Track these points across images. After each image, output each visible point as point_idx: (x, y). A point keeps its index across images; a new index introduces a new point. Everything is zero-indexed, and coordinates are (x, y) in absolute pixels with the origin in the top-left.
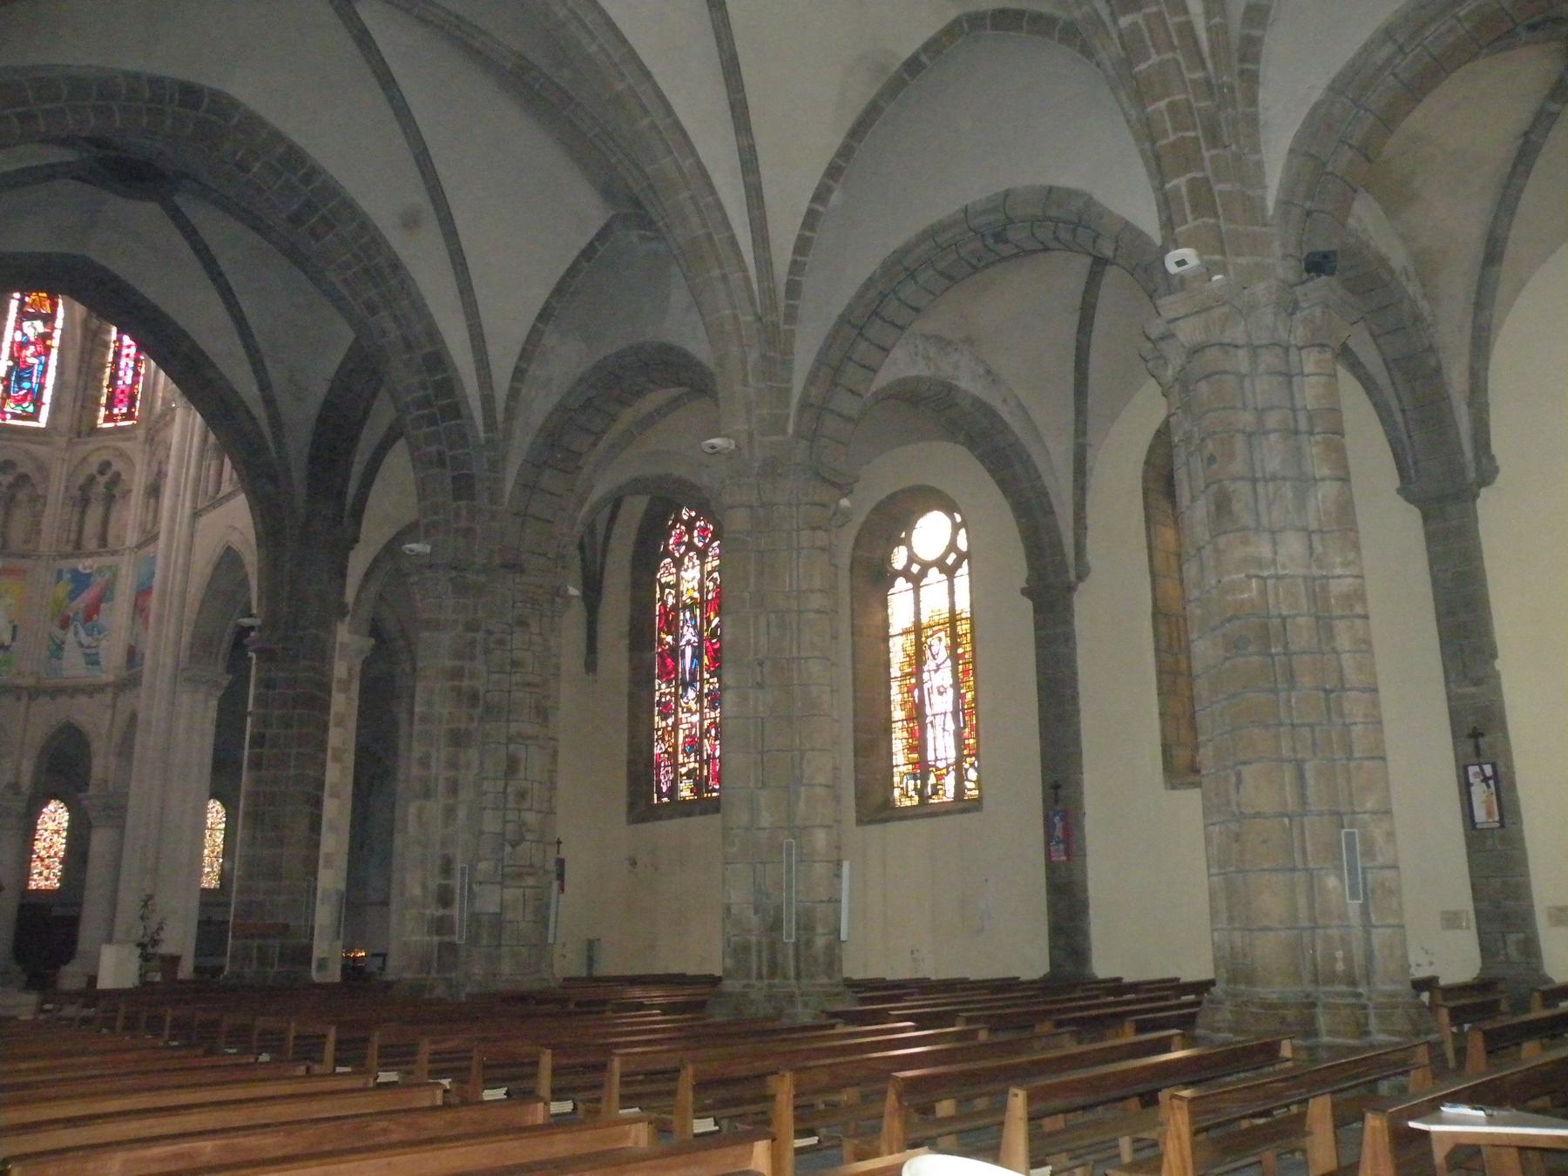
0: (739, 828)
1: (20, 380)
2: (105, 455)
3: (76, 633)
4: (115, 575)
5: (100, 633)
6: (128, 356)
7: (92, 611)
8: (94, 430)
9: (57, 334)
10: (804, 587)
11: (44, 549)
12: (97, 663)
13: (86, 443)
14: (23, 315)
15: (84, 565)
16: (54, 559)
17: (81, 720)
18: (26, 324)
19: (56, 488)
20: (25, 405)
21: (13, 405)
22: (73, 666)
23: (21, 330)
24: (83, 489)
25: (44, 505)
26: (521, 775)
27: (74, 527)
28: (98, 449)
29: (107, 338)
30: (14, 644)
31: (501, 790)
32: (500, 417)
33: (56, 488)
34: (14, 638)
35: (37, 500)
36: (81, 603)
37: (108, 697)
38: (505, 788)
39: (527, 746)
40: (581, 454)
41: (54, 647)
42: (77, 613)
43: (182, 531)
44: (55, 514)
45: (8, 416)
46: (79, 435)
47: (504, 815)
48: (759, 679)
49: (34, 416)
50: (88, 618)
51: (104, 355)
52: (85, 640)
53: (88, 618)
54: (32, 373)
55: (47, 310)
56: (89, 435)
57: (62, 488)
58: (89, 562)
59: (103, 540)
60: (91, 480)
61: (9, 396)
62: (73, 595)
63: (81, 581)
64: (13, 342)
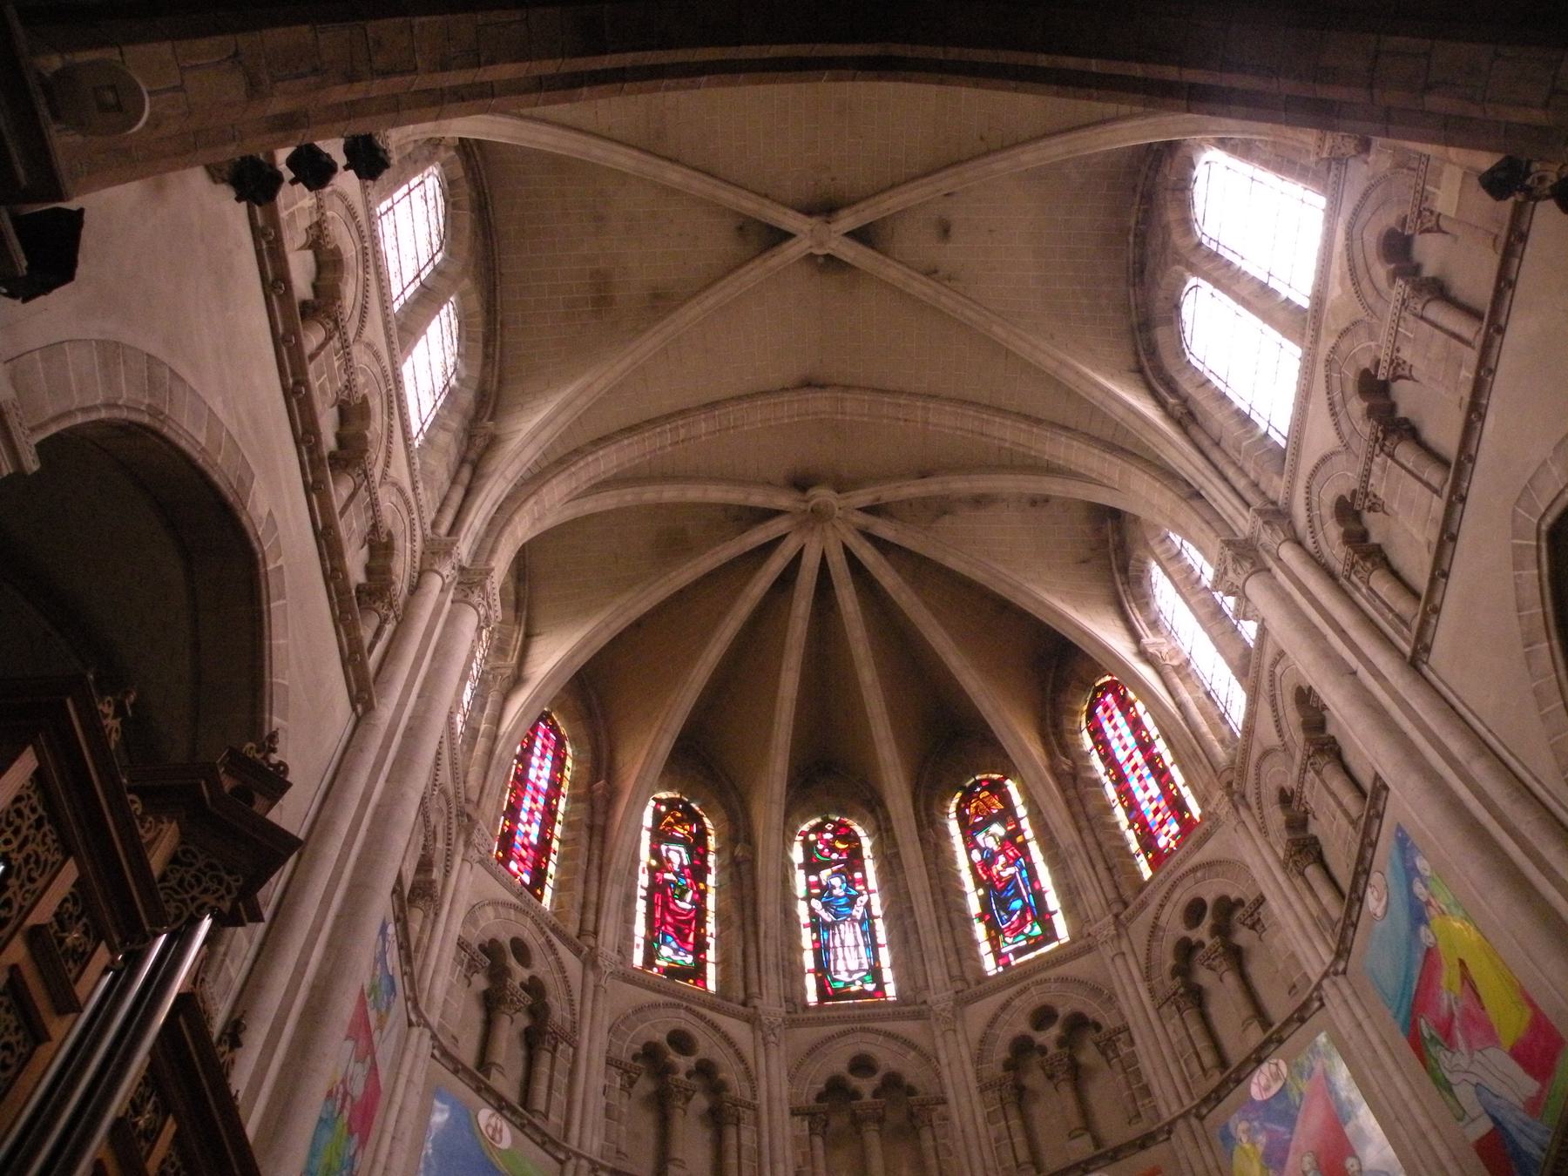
1: (1004, 904)
6: (1135, 768)
9: (1025, 824)
11: (1169, 1108)
14: (969, 831)
16: (1201, 1118)
18: (980, 838)
20: (1026, 930)
21: (1009, 940)
23: (977, 846)
25: (1132, 1042)
27: (1202, 1044)
29: (1095, 776)
35: (1113, 1041)
43: (1418, 702)
45: (1011, 957)
49: (1049, 934)
51: (1101, 795)
54: (1017, 887)
55: (997, 807)
57: (1145, 996)
61: (1000, 931)
64: (973, 867)
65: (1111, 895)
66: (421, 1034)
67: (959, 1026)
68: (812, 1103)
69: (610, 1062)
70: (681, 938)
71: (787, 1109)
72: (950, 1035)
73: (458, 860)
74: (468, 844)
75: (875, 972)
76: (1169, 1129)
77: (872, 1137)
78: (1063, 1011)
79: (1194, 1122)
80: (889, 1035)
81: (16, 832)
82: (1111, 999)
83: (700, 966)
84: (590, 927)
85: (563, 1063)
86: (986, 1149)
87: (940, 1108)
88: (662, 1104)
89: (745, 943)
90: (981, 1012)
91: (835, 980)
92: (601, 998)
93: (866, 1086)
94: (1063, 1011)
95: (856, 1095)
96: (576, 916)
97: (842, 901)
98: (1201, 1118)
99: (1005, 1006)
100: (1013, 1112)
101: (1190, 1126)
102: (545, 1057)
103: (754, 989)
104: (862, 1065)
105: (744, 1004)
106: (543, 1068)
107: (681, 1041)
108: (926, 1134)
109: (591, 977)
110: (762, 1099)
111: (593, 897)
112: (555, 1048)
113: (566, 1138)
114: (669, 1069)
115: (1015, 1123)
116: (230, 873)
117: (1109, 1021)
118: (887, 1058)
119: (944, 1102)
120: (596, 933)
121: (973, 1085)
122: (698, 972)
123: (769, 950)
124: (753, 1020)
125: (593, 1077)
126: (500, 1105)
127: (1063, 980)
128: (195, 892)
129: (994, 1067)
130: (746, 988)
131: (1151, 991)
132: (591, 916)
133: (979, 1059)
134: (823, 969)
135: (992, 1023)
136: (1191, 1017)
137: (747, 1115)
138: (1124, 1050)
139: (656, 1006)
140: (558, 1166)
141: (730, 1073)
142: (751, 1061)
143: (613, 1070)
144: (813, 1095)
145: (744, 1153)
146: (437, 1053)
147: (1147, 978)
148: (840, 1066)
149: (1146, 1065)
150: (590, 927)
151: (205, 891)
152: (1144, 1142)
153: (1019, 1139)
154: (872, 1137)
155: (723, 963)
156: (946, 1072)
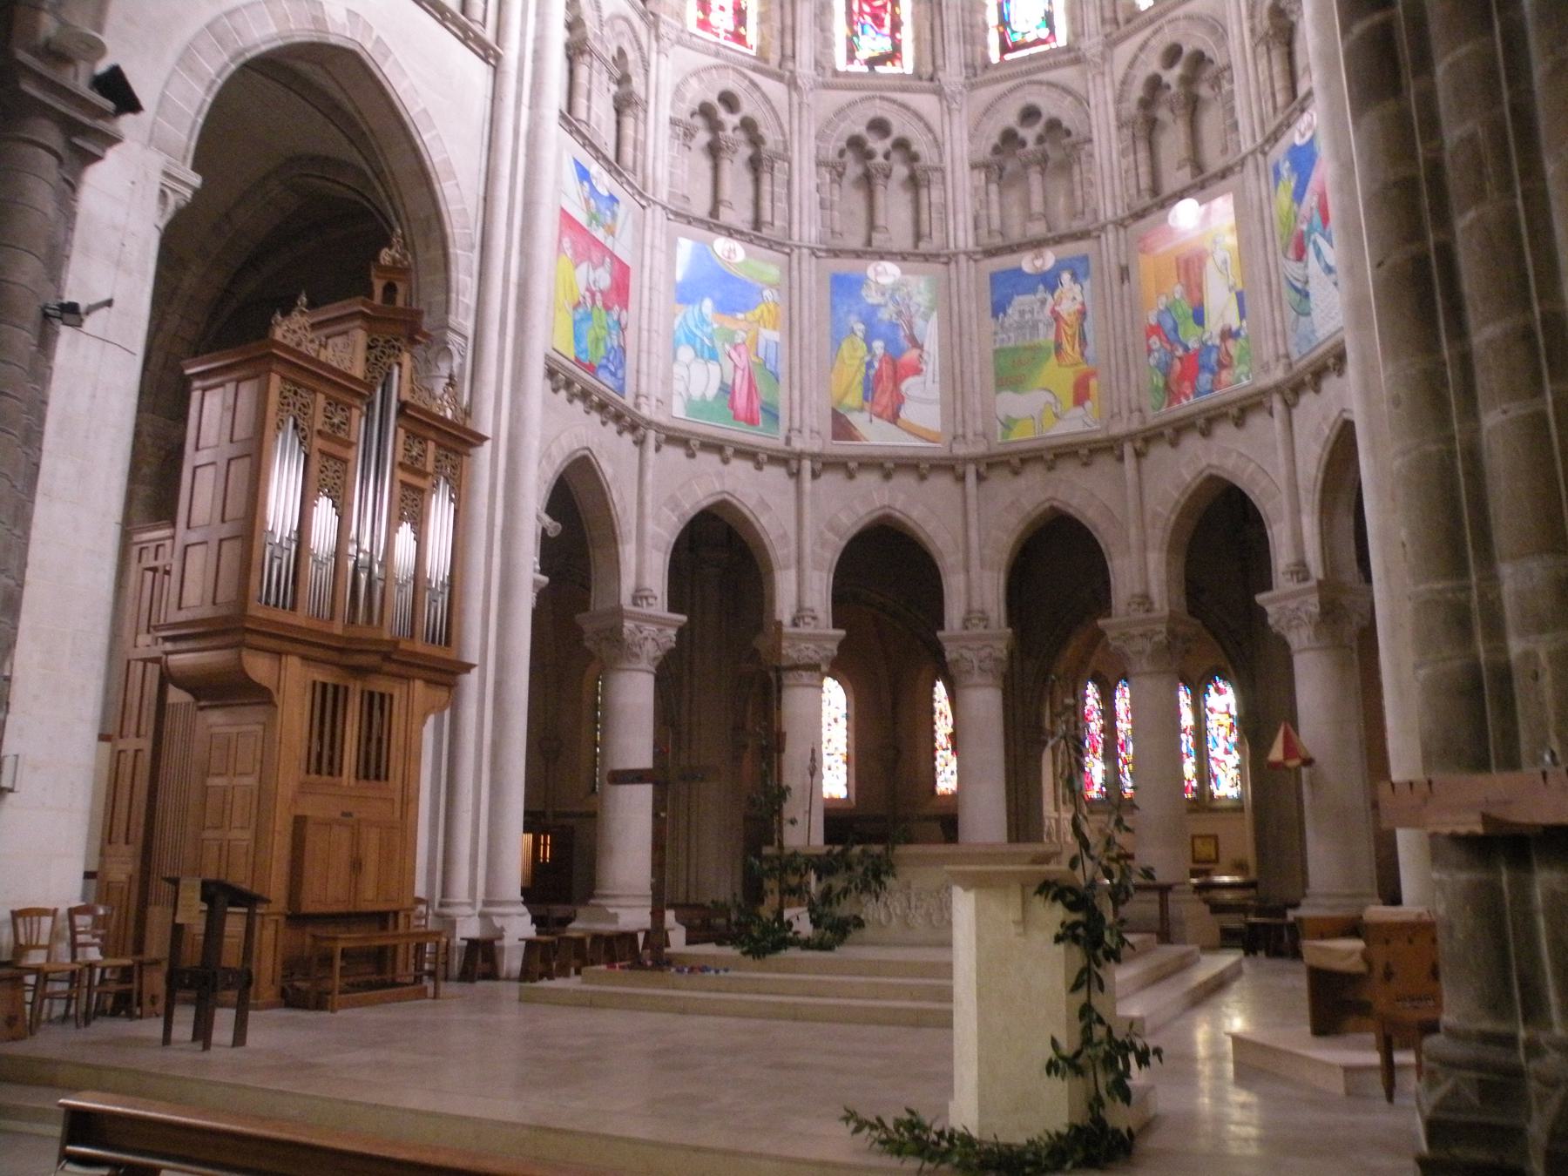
16: (1265, 154)
25: (1231, 81)
30: (1244, 323)
34: (1242, 315)
41: (1295, 296)
42: (1310, 222)
57: (1247, 34)
62: (1298, 196)
66: (653, 211)
67: (1107, 68)
68: (988, 156)
70: (878, 21)
71: (967, 167)
72: (1099, 79)
73: (653, 58)
74: (658, 38)
75: (1049, 19)
77: (1035, 178)
78: (1187, 49)
79: (1260, 157)
80: (1051, 84)
81: (288, 405)
83: (897, 47)
84: (789, 52)
85: (780, 177)
86: (1117, 182)
87: (1087, 147)
89: (933, 19)
91: (1013, 32)
92: (805, 113)
93: (1029, 134)
94: (1187, 49)
95: (1023, 143)
96: (776, 44)
98: (1265, 154)
100: (1142, 148)
101: (1256, 160)
102: (766, 179)
103: (939, 62)
104: (1030, 114)
105: (931, 79)
106: (766, 187)
107: (879, 126)
108: (1076, 169)
109: (795, 96)
111: (789, 21)
112: (772, 168)
114: (870, 155)
115: (1143, 155)
116: (396, 340)
117: (1220, 61)
118: (1050, 106)
119: (1090, 141)
121: (1113, 123)
122: (893, 56)
124: (939, 92)
125: (806, 177)
127: (1189, 17)
128: (385, 359)
129: (1131, 106)
131: (1253, 30)
132: (788, 40)
133: (1119, 99)
134: (1004, 22)
135: (1132, 65)
136: (1277, 54)
137: (935, 177)
138: (1226, 87)
139: (852, 104)
140: (787, 257)
141: (921, 145)
142: (937, 130)
143: (823, 170)
144: (989, 149)
145: (933, 209)
146: (671, 217)
149: (1239, 102)
150: (789, 52)
151: (389, 357)
153: (1143, 169)
154: (1035, 178)
156: (1093, 113)
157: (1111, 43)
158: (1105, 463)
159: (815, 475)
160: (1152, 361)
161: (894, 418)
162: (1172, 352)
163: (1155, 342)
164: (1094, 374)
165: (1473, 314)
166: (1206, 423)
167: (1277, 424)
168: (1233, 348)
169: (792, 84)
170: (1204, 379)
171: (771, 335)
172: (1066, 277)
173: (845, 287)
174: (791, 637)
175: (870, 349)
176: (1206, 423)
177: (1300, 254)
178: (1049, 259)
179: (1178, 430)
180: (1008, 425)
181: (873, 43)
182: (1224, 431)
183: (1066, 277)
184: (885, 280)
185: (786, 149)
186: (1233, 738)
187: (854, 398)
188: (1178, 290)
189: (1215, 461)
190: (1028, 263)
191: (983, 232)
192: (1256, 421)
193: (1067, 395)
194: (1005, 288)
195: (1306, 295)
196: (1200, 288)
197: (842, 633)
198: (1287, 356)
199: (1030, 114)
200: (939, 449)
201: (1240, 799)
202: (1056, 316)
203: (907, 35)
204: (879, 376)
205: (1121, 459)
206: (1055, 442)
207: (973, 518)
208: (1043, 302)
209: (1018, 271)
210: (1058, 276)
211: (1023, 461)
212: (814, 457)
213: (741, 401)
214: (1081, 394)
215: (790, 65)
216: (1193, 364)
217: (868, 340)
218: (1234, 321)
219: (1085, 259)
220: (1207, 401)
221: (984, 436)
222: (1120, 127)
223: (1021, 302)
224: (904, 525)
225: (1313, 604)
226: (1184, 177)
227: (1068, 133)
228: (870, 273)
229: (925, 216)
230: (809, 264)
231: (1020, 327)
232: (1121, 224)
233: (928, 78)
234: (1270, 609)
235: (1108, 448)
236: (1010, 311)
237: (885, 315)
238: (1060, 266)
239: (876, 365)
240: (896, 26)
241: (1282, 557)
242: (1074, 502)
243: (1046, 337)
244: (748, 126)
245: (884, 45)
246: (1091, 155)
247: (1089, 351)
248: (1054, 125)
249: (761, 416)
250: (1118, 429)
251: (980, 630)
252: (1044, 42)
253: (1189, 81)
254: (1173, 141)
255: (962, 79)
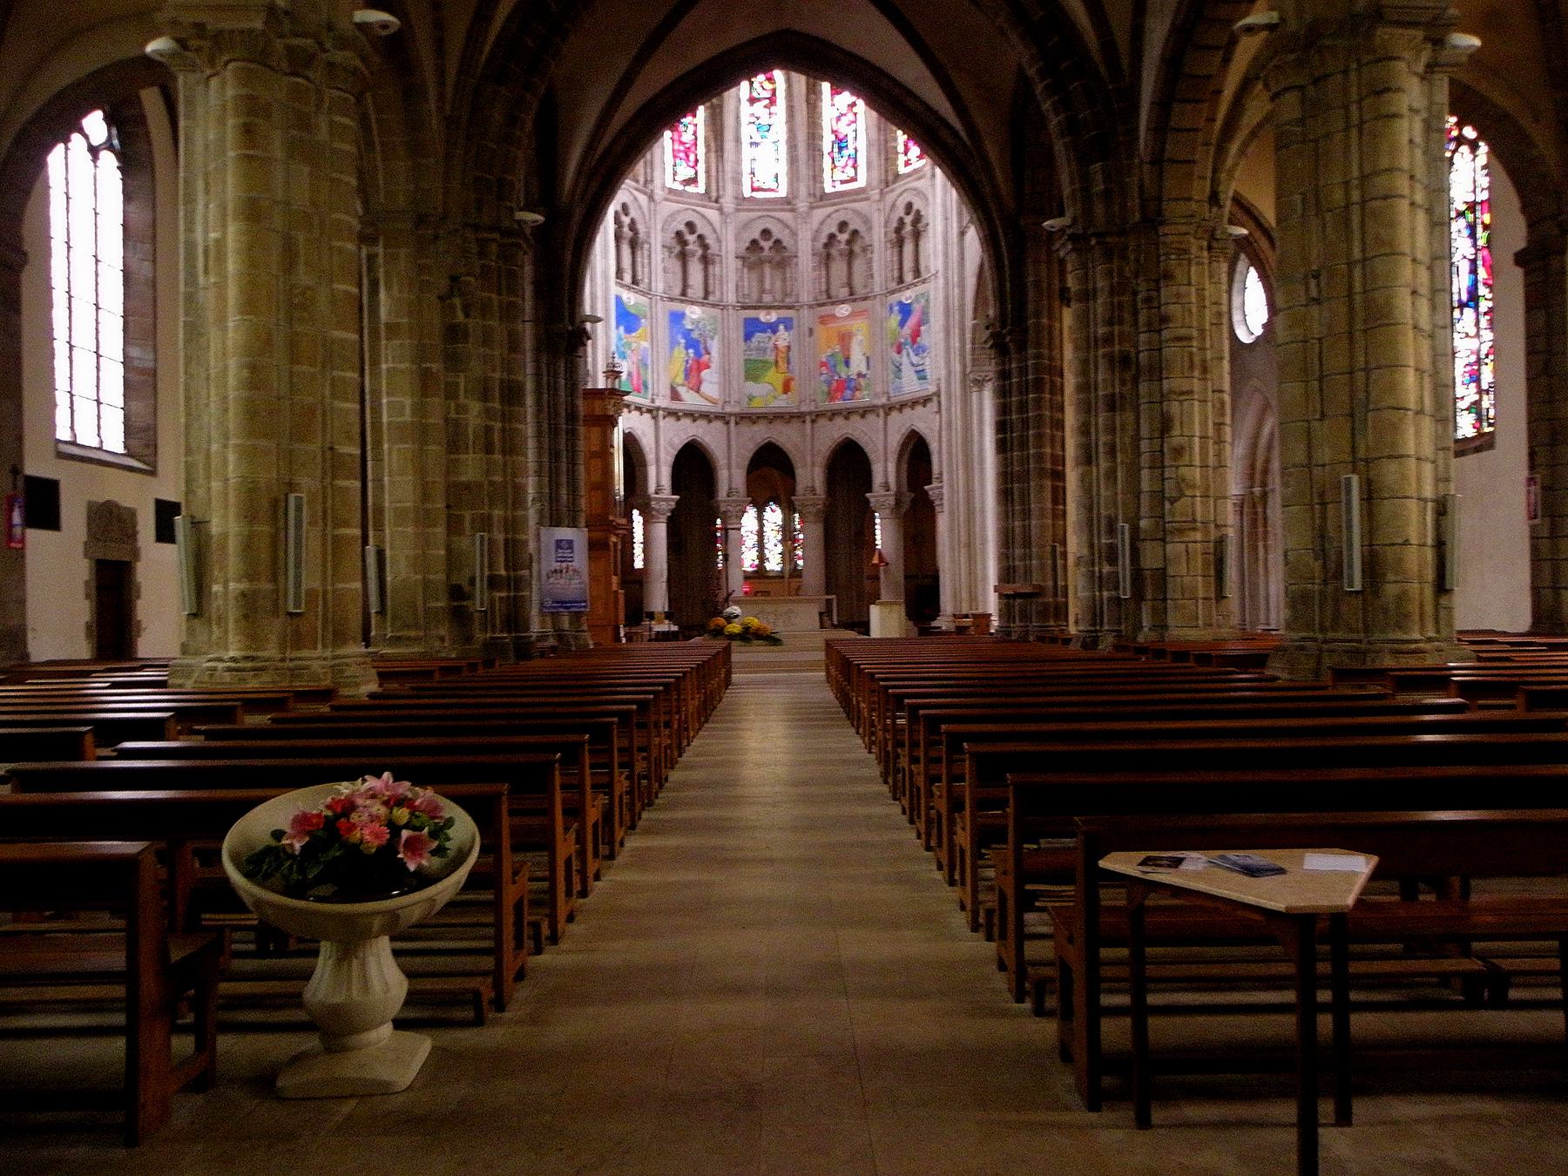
0: (1294, 466)
1: (840, 149)
2: (907, 197)
3: (908, 355)
4: (927, 301)
5: (924, 352)
7: (916, 334)
8: (897, 176)
10: (1367, 170)
11: (877, 289)
12: (924, 378)
13: (892, 191)
15: (906, 296)
17: (921, 427)
19: (878, 237)
22: (910, 386)
24: (898, 230)
26: (1176, 431)
28: (901, 194)
31: (1157, 448)
32: (1125, 62)
33: (878, 237)
36: (907, 330)
37: (932, 406)
38: (1162, 446)
39: (1181, 401)
40: (1209, 77)
44: (881, 256)
46: (887, 186)
47: (1162, 475)
48: (1314, 293)
50: (914, 341)
52: (915, 359)
53: (914, 341)
56: (894, 183)
57: (883, 235)
58: (908, 293)
59: (917, 272)
60: (901, 222)
62: (902, 324)
63: (905, 310)
65: (883, 177)
69: (664, 246)
76: (875, 296)
77: (767, 270)
78: (852, 227)
80: (779, 220)
82: (870, 229)
85: (646, 253)
87: (795, 260)
88: (683, 257)
90: (820, 214)
93: (766, 245)
94: (852, 227)
95: (762, 249)
97: (766, 128)
99: (829, 216)
100: (823, 269)
102: (639, 253)
103: (721, 193)
104: (766, 233)
108: (788, 270)
110: (723, 253)
113: (650, 290)
115: (824, 272)
117: (867, 241)
118: (777, 232)
119: (796, 257)
120: (652, 181)
123: (729, 166)
124: (720, 210)
126: (629, 288)
127: (855, 211)
129: (819, 245)
130: (718, 190)
133: (814, 240)
136: (896, 250)
137: (717, 259)
138: (869, 256)
139: (678, 212)
141: (710, 241)
147: (886, 226)
148: (756, 235)
149: (875, 265)
152: (865, 299)
153: (823, 280)
154: (767, 270)
155: (708, 172)
157: (812, 208)
158: (796, 424)
159: (664, 418)
160: (822, 379)
161: (698, 391)
162: (833, 376)
163: (824, 370)
164: (793, 379)
165: (1016, 503)
166: (848, 414)
167: (881, 422)
168: (862, 381)
169: (651, 198)
170: (848, 393)
171: (645, 344)
172: (781, 327)
173: (677, 318)
174: (656, 499)
175: (687, 354)
176: (848, 414)
177: (899, 352)
178: (773, 317)
179: (834, 414)
180: (751, 398)
181: (685, 172)
182: (855, 418)
183: (781, 327)
184: (694, 317)
185: (649, 237)
186: (780, 537)
187: (680, 379)
188: (838, 348)
189: (850, 432)
190: (764, 317)
191: (740, 294)
192: (871, 417)
193: (780, 389)
194: (752, 328)
195: (900, 370)
196: (848, 349)
197: (677, 497)
198: (888, 393)
199: (766, 233)
200: (717, 409)
201: (781, 572)
202: (776, 347)
203: (701, 167)
204: (691, 367)
205: (804, 422)
206: (774, 410)
207: (733, 443)
208: (770, 338)
209: (757, 319)
210: (777, 326)
211: (758, 418)
212: (664, 409)
213: (635, 382)
214: (786, 388)
215: (650, 187)
216: (843, 386)
217: (687, 348)
218: (864, 370)
219: (791, 319)
220: (849, 404)
221: (739, 403)
222: (813, 255)
223: (758, 336)
224: (700, 444)
225: (892, 501)
226: (844, 292)
227: (785, 248)
228: (687, 312)
229: (711, 281)
230: (660, 304)
231: (758, 349)
232: (811, 307)
233: (712, 197)
234: (872, 500)
235: (800, 416)
236: (753, 340)
237: (695, 335)
238: (779, 321)
239: (690, 362)
240: (697, 161)
241: (878, 479)
242: (782, 440)
243: (771, 357)
244: (633, 224)
245: (690, 173)
246: (797, 264)
247: (791, 367)
248: (778, 242)
249: (642, 387)
250: (804, 409)
251: (734, 498)
252: (772, 190)
253: (849, 242)
254: (839, 268)
255: (733, 206)
